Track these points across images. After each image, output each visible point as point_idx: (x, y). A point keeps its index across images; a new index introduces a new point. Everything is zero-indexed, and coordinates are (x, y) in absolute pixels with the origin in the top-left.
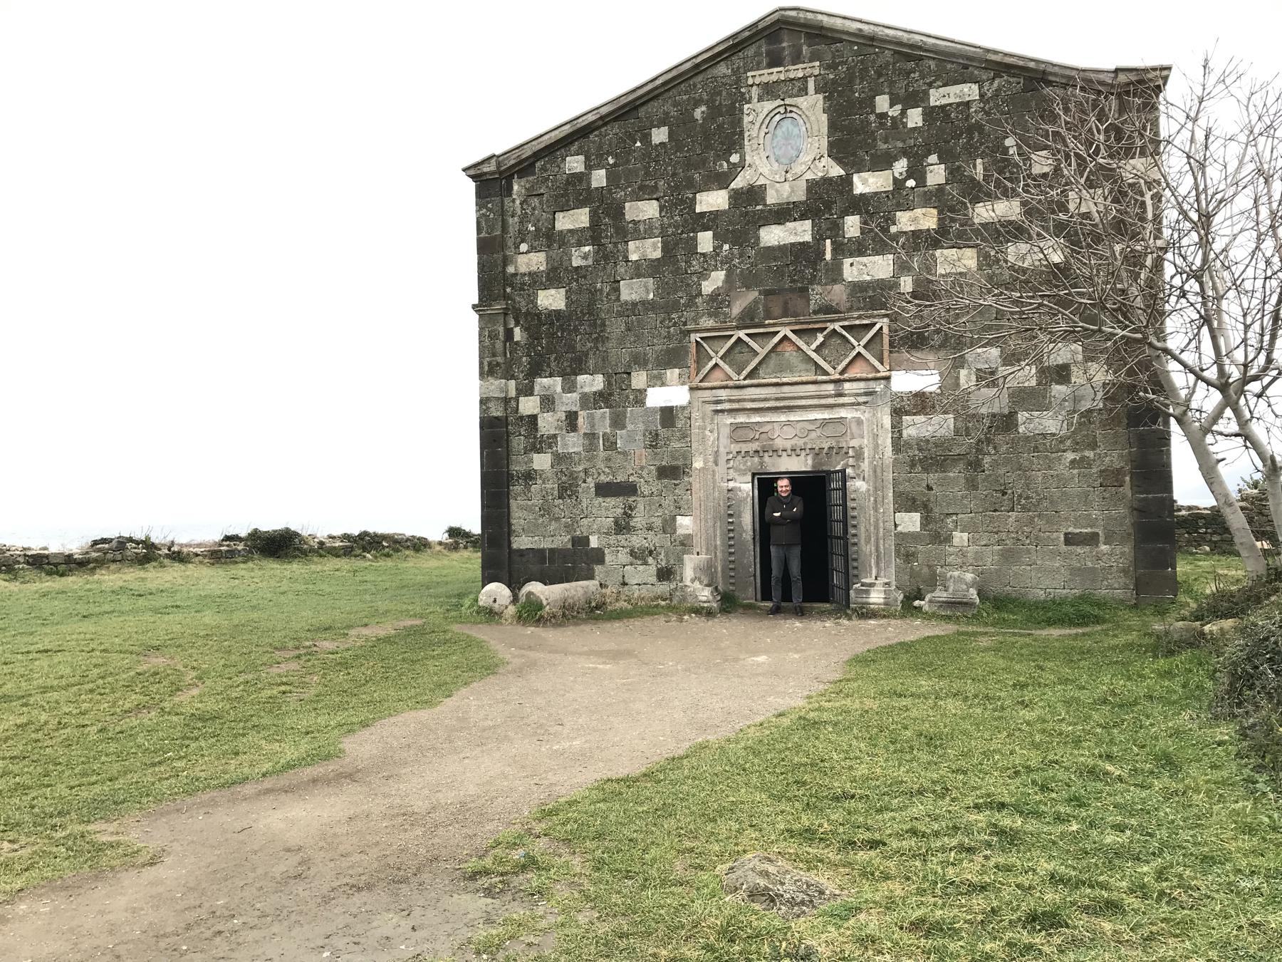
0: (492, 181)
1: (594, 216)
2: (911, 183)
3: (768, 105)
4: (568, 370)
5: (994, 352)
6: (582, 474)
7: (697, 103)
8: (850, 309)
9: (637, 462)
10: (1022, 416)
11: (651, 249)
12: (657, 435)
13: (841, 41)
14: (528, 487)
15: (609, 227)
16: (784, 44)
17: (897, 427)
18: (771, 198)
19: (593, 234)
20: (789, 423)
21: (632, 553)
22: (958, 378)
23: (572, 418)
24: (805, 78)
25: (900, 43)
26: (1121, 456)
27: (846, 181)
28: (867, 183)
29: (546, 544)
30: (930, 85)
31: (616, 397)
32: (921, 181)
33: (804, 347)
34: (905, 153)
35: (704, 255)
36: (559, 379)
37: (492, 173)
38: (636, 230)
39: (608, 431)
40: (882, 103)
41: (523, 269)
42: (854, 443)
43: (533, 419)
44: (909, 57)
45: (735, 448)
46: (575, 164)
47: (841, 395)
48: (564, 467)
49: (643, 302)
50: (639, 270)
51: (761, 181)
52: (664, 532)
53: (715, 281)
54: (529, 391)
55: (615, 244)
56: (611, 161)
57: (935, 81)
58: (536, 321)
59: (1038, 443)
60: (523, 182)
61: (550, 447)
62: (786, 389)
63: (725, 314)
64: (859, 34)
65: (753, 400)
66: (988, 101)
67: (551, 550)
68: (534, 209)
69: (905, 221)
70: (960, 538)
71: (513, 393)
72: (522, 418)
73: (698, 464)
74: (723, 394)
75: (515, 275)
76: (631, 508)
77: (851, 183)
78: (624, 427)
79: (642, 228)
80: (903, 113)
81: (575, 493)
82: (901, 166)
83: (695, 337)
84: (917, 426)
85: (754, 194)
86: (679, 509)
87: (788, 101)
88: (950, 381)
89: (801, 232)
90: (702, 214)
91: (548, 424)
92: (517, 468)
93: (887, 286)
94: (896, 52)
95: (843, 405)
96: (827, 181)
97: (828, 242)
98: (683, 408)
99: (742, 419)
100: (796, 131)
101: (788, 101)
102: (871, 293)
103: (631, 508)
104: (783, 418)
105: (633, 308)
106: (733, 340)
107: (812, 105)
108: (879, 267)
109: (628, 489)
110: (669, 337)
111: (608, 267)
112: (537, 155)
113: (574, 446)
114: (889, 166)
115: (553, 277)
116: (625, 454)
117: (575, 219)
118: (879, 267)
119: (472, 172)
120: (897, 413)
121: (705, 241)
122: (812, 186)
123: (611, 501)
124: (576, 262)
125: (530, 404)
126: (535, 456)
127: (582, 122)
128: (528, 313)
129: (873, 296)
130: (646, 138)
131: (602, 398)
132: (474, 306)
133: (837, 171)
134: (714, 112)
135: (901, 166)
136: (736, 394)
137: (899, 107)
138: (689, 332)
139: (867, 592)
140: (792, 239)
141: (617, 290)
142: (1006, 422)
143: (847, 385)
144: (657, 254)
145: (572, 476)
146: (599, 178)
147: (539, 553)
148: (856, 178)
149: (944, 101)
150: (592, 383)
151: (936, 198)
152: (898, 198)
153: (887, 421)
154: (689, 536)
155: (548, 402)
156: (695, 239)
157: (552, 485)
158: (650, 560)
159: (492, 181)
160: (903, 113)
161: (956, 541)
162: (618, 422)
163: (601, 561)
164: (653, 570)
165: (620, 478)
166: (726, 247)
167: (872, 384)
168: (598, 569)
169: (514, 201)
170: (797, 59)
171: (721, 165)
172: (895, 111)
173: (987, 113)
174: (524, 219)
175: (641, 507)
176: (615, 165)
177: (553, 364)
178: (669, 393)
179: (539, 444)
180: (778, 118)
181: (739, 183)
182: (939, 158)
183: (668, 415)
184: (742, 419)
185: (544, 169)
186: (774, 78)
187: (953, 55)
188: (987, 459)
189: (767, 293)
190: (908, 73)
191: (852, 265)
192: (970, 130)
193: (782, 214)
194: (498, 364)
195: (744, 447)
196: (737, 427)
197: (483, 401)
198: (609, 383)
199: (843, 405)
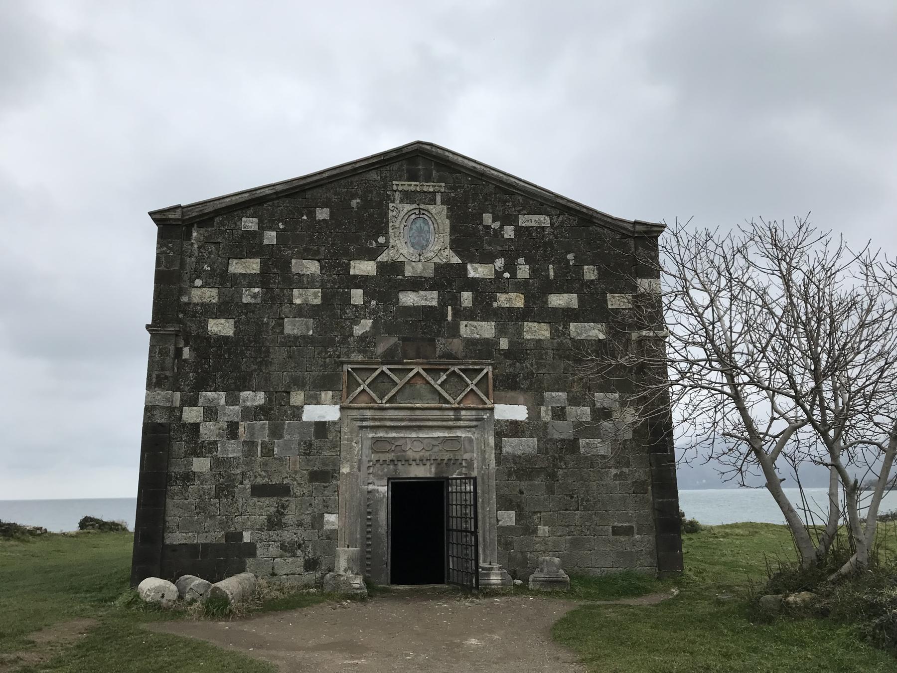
0: (174, 226)
1: (263, 265)
2: (507, 275)
3: (407, 207)
4: (233, 386)
5: (563, 395)
6: (240, 477)
7: (354, 196)
8: (465, 357)
10: (582, 442)
11: (314, 297)
12: (311, 445)
13: (460, 172)
14: (185, 487)
15: (276, 275)
16: (420, 167)
17: (498, 446)
18: (409, 272)
19: (262, 279)
20: (418, 439)
21: (283, 547)
22: (539, 412)
24: (434, 193)
26: (645, 472)
27: (463, 268)
28: (476, 271)
29: (200, 540)
30: (519, 212)
31: (278, 411)
32: (514, 274)
33: (432, 382)
34: (502, 254)
35: (356, 306)
36: (223, 394)
37: (178, 220)
39: (267, 439)
40: (487, 218)
41: (196, 300)
42: (467, 456)
43: (196, 426)
44: (506, 192)
45: (374, 457)
46: (250, 224)
48: (222, 470)
49: (304, 337)
50: (301, 311)
51: (402, 259)
52: (313, 527)
53: (364, 326)
54: (194, 403)
55: (282, 289)
56: (281, 226)
57: (522, 210)
58: (206, 344)
59: (591, 461)
60: (202, 231)
61: (210, 452)
62: (418, 412)
63: (372, 352)
64: (473, 170)
65: (392, 420)
66: (556, 229)
67: (205, 546)
68: (210, 253)
69: (503, 300)
70: (543, 530)
71: (178, 403)
72: (184, 425)
73: (345, 470)
74: (369, 414)
75: (188, 304)
76: (283, 507)
77: (466, 269)
78: (281, 437)
79: (305, 280)
80: (501, 227)
82: (500, 263)
83: (349, 367)
84: (511, 445)
85: (396, 267)
86: (328, 508)
87: (422, 206)
88: (534, 414)
89: (430, 299)
90: (356, 276)
91: (209, 431)
92: (177, 469)
94: (497, 187)
95: (459, 427)
96: (448, 265)
97: (450, 308)
98: (334, 423)
99: (381, 434)
100: (426, 228)
101: (422, 206)
102: (479, 347)
103: (283, 507)
104: (414, 435)
106: (378, 372)
107: (439, 210)
108: (486, 329)
109: (283, 491)
110: (325, 365)
111: (275, 307)
112: (218, 212)
113: (233, 451)
114: (493, 262)
115: (222, 310)
118: (486, 329)
119: (158, 216)
120: (499, 435)
121: (357, 296)
122: (438, 267)
123: (266, 501)
125: (194, 414)
126: (195, 459)
128: (198, 336)
131: (263, 411)
132: (148, 327)
133: (456, 260)
134: (366, 204)
135: (500, 263)
136: (379, 414)
137: (498, 223)
138: (343, 363)
139: (488, 575)
140: (423, 303)
142: (572, 445)
143: (463, 413)
144: (318, 301)
145: (231, 479)
147: (192, 549)
148: (469, 266)
149: (528, 224)
151: (521, 286)
152: (498, 284)
153: (492, 441)
154: (334, 532)
155: (211, 413)
156: (349, 294)
157: (209, 486)
158: (299, 552)
159: (173, 225)
160: (501, 227)
161: (540, 533)
162: (276, 432)
164: (300, 561)
165: (275, 481)
167: (481, 413)
168: (249, 561)
169: (192, 244)
170: (428, 179)
171: (371, 243)
172: (496, 225)
173: (556, 236)
174: (200, 260)
176: (284, 230)
177: (218, 381)
179: (199, 449)
180: (413, 217)
181: (383, 257)
182: (525, 260)
183: (321, 427)
184: (381, 434)
185: (222, 223)
186: (412, 188)
188: (560, 472)
189: (404, 340)
190: (505, 202)
191: (466, 326)
192: (545, 245)
193: (416, 284)
194: (166, 377)
195: (382, 457)
196: (377, 440)
197: (148, 409)
199: (459, 427)
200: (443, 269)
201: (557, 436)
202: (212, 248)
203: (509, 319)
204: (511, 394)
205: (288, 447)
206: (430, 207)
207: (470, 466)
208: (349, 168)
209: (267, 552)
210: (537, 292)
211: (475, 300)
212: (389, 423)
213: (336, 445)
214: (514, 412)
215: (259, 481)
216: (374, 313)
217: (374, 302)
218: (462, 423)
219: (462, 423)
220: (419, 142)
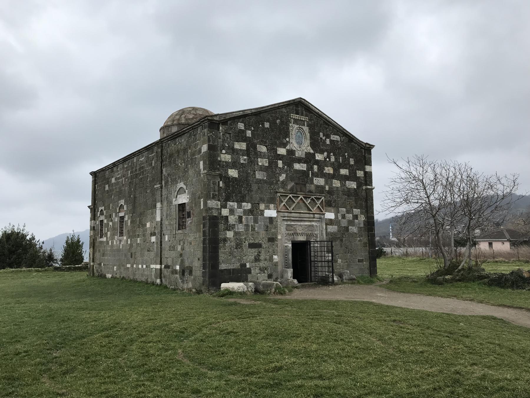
1: (247, 146)
5: (344, 209)
7: (277, 118)
8: (315, 192)
9: (262, 237)
10: (350, 227)
13: (312, 113)
15: (251, 152)
17: (326, 229)
19: (247, 152)
20: (301, 225)
21: (260, 269)
23: (240, 218)
25: (326, 120)
28: (319, 157)
29: (231, 267)
31: (255, 212)
34: (326, 151)
37: (216, 121)
38: (261, 155)
41: (223, 160)
42: (316, 233)
43: (227, 217)
44: (327, 124)
45: (287, 232)
47: (314, 218)
49: (263, 180)
50: (262, 169)
51: (294, 149)
53: (282, 177)
58: (227, 180)
60: (224, 127)
62: (302, 214)
64: (318, 113)
65: (293, 217)
67: (233, 269)
68: (227, 138)
72: (222, 217)
73: (279, 237)
74: (286, 214)
76: (260, 252)
78: (258, 223)
81: (241, 247)
82: (326, 154)
86: (275, 253)
87: (301, 126)
91: (232, 219)
92: (221, 237)
93: (323, 187)
94: (324, 122)
98: (275, 218)
99: (289, 223)
101: (301, 126)
103: (260, 252)
104: (299, 224)
105: (259, 181)
106: (289, 197)
107: (306, 129)
112: (230, 119)
113: (241, 229)
114: (323, 154)
115: (234, 165)
116: (258, 233)
117: (241, 146)
120: (326, 224)
121: (280, 163)
123: (254, 250)
124: (242, 162)
125: (226, 212)
127: (246, 112)
128: (225, 177)
129: (320, 189)
130: (263, 125)
133: (312, 151)
134: (282, 122)
135: (326, 154)
136: (289, 214)
138: (277, 192)
140: (301, 169)
141: (255, 174)
142: (347, 229)
143: (316, 215)
144: (267, 165)
146: (249, 133)
147: (228, 271)
150: (247, 206)
151: (332, 165)
154: (277, 262)
155: (232, 212)
156: (277, 162)
158: (266, 271)
161: (338, 262)
162: (256, 221)
163: (250, 273)
164: (266, 275)
165: (257, 242)
166: (286, 167)
167: (321, 215)
169: (220, 133)
172: (324, 138)
174: (224, 141)
175: (263, 252)
176: (253, 130)
177: (234, 197)
178: (271, 213)
179: (229, 227)
183: (271, 219)
184: (289, 223)
185: (231, 124)
187: (337, 127)
188: (344, 239)
189: (296, 184)
190: (327, 128)
193: (299, 160)
194: (216, 195)
196: (288, 225)
198: (252, 207)
200: (307, 154)
201: (343, 225)
202: (228, 135)
203: (329, 178)
204: (329, 208)
205: (260, 227)
206: (303, 127)
207: (317, 237)
208: (277, 106)
209: (255, 271)
210: (337, 167)
211: (318, 169)
212: (292, 219)
213: (276, 227)
214: (330, 215)
215: (251, 242)
216: (286, 171)
217: (286, 167)
218: (315, 219)
219: (315, 219)
220: (301, 98)
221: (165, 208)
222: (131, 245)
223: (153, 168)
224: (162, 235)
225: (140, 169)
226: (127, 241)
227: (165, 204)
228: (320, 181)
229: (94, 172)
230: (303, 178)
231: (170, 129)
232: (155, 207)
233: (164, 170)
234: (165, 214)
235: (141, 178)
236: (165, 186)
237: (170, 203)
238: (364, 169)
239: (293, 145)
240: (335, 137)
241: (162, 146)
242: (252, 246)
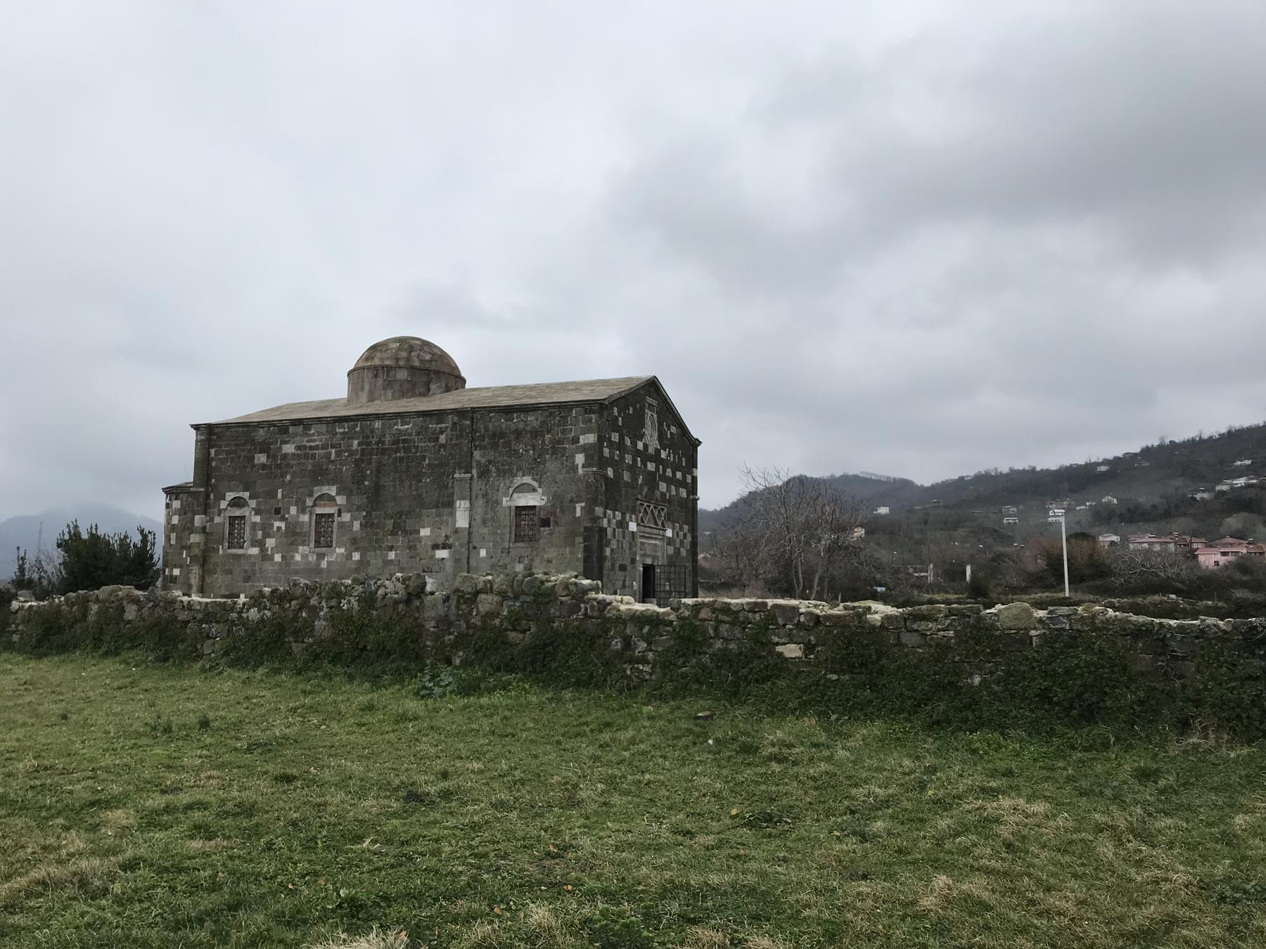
31: (623, 524)
117: (615, 437)
155: (609, 521)
221: (480, 510)
222: (363, 563)
223: (443, 446)
224: (471, 547)
225: (396, 442)
226: (349, 557)
227: (480, 502)
228: (663, 487)
229: (209, 425)
230: (652, 479)
231: (392, 373)
232: (450, 504)
233: (477, 454)
234: (478, 518)
235: (401, 459)
236: (479, 477)
237: (492, 503)
238: (691, 473)
239: (647, 439)
240: (673, 429)
241: (472, 418)
242: (623, 568)
